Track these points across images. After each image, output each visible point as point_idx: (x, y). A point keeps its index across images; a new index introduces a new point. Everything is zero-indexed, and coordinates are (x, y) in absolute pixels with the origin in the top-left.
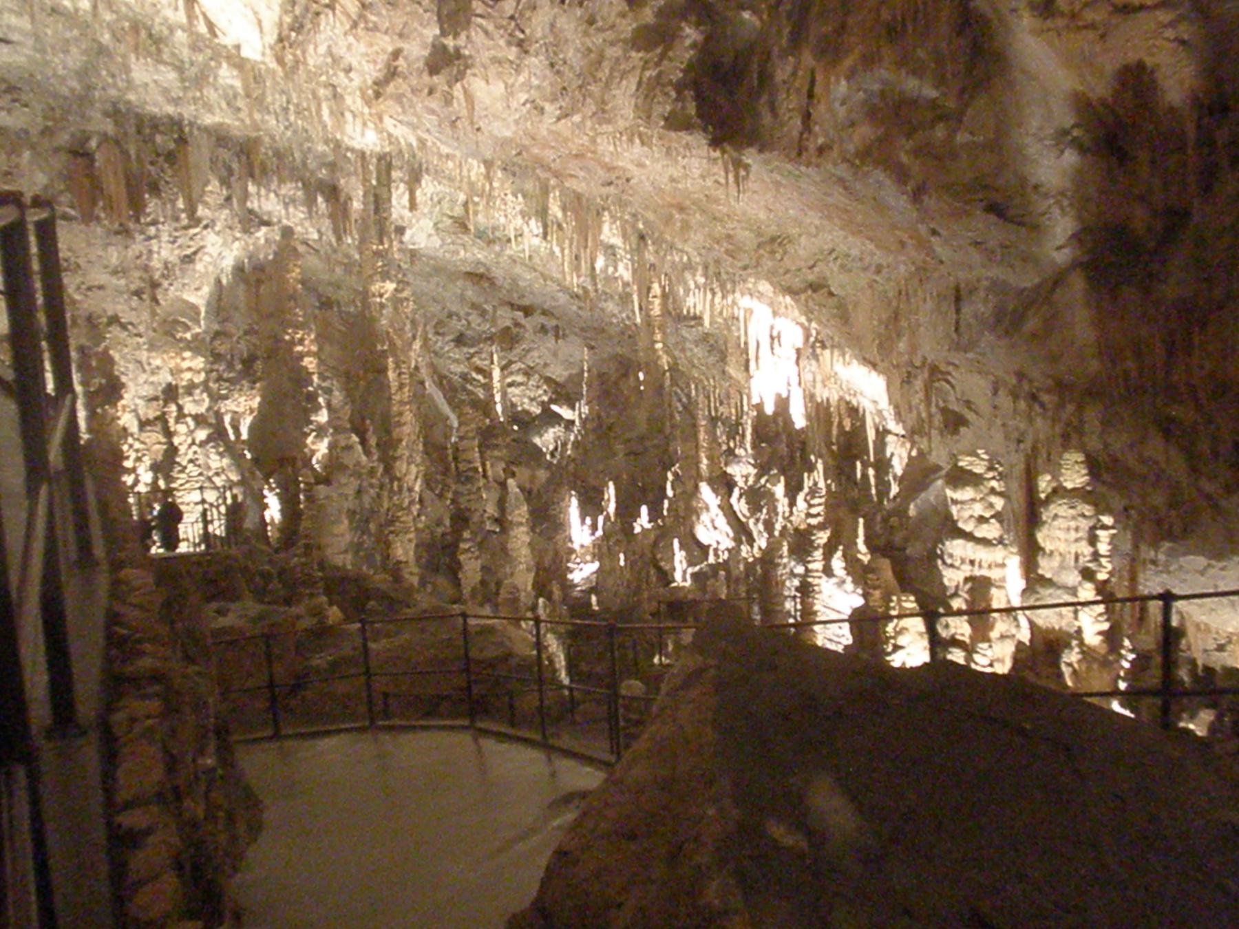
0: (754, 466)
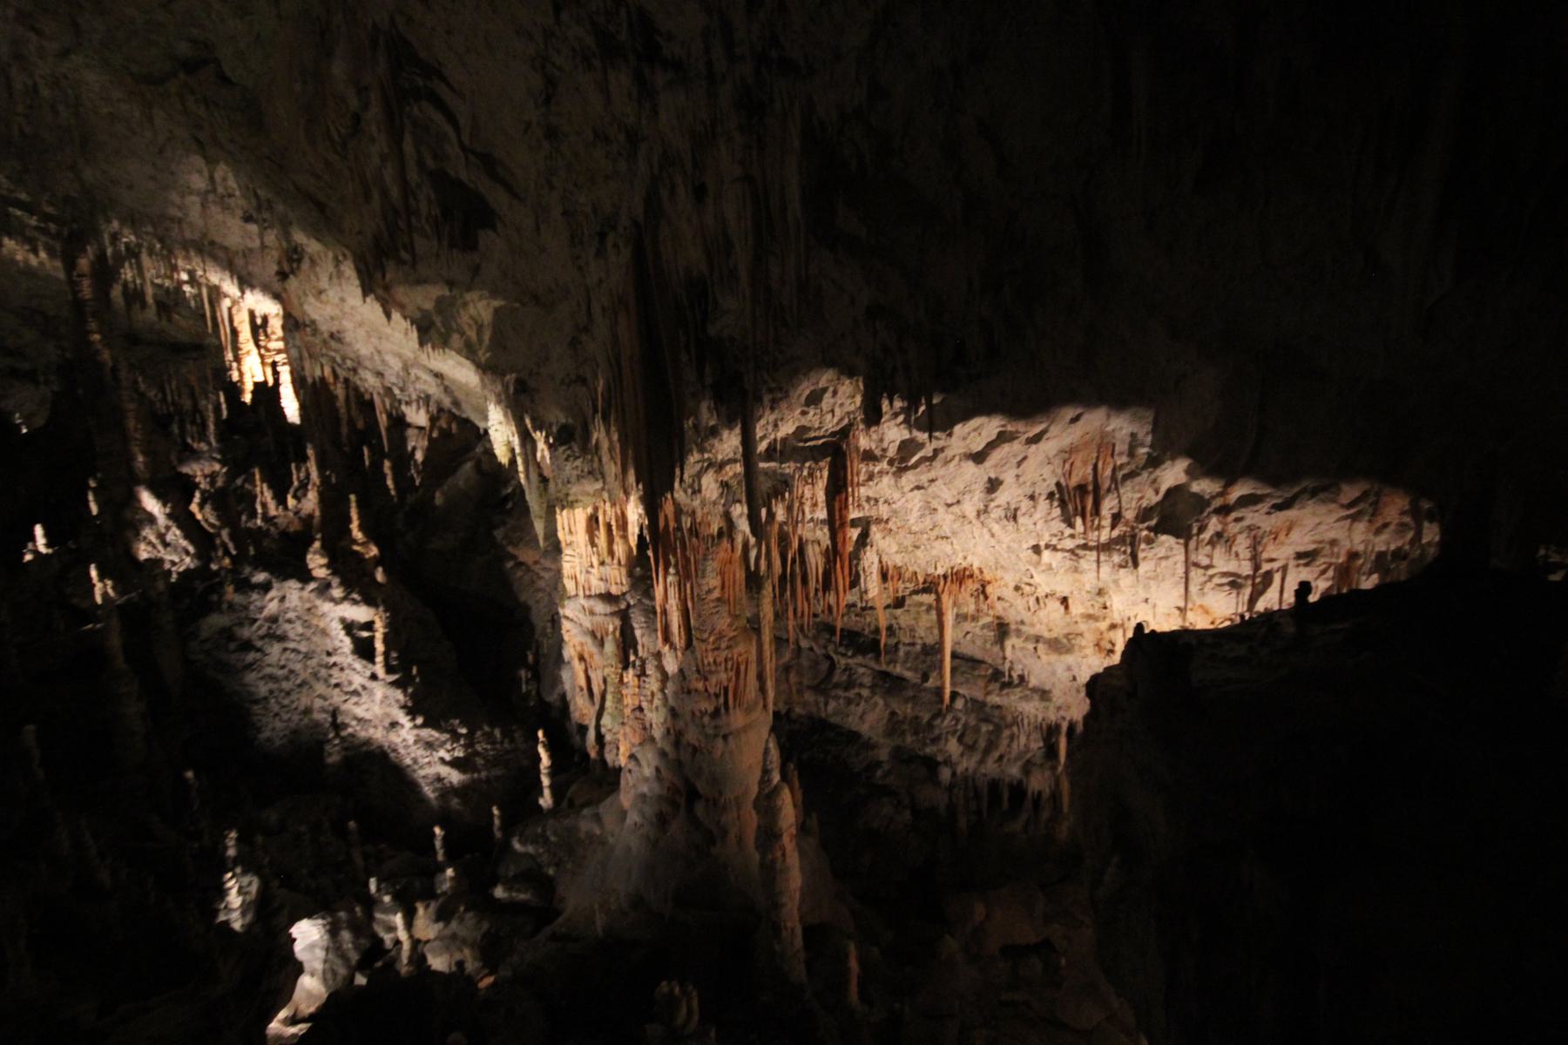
0: (219, 461)
